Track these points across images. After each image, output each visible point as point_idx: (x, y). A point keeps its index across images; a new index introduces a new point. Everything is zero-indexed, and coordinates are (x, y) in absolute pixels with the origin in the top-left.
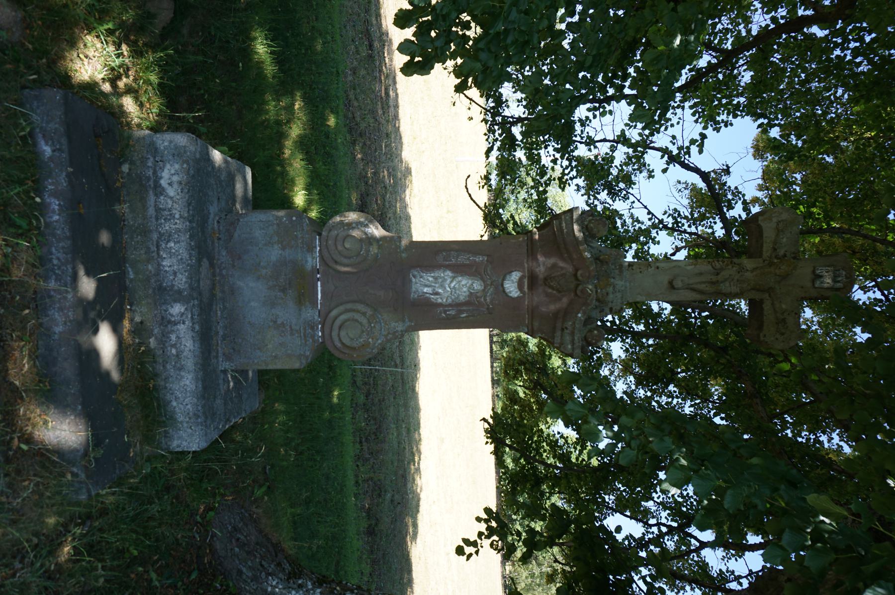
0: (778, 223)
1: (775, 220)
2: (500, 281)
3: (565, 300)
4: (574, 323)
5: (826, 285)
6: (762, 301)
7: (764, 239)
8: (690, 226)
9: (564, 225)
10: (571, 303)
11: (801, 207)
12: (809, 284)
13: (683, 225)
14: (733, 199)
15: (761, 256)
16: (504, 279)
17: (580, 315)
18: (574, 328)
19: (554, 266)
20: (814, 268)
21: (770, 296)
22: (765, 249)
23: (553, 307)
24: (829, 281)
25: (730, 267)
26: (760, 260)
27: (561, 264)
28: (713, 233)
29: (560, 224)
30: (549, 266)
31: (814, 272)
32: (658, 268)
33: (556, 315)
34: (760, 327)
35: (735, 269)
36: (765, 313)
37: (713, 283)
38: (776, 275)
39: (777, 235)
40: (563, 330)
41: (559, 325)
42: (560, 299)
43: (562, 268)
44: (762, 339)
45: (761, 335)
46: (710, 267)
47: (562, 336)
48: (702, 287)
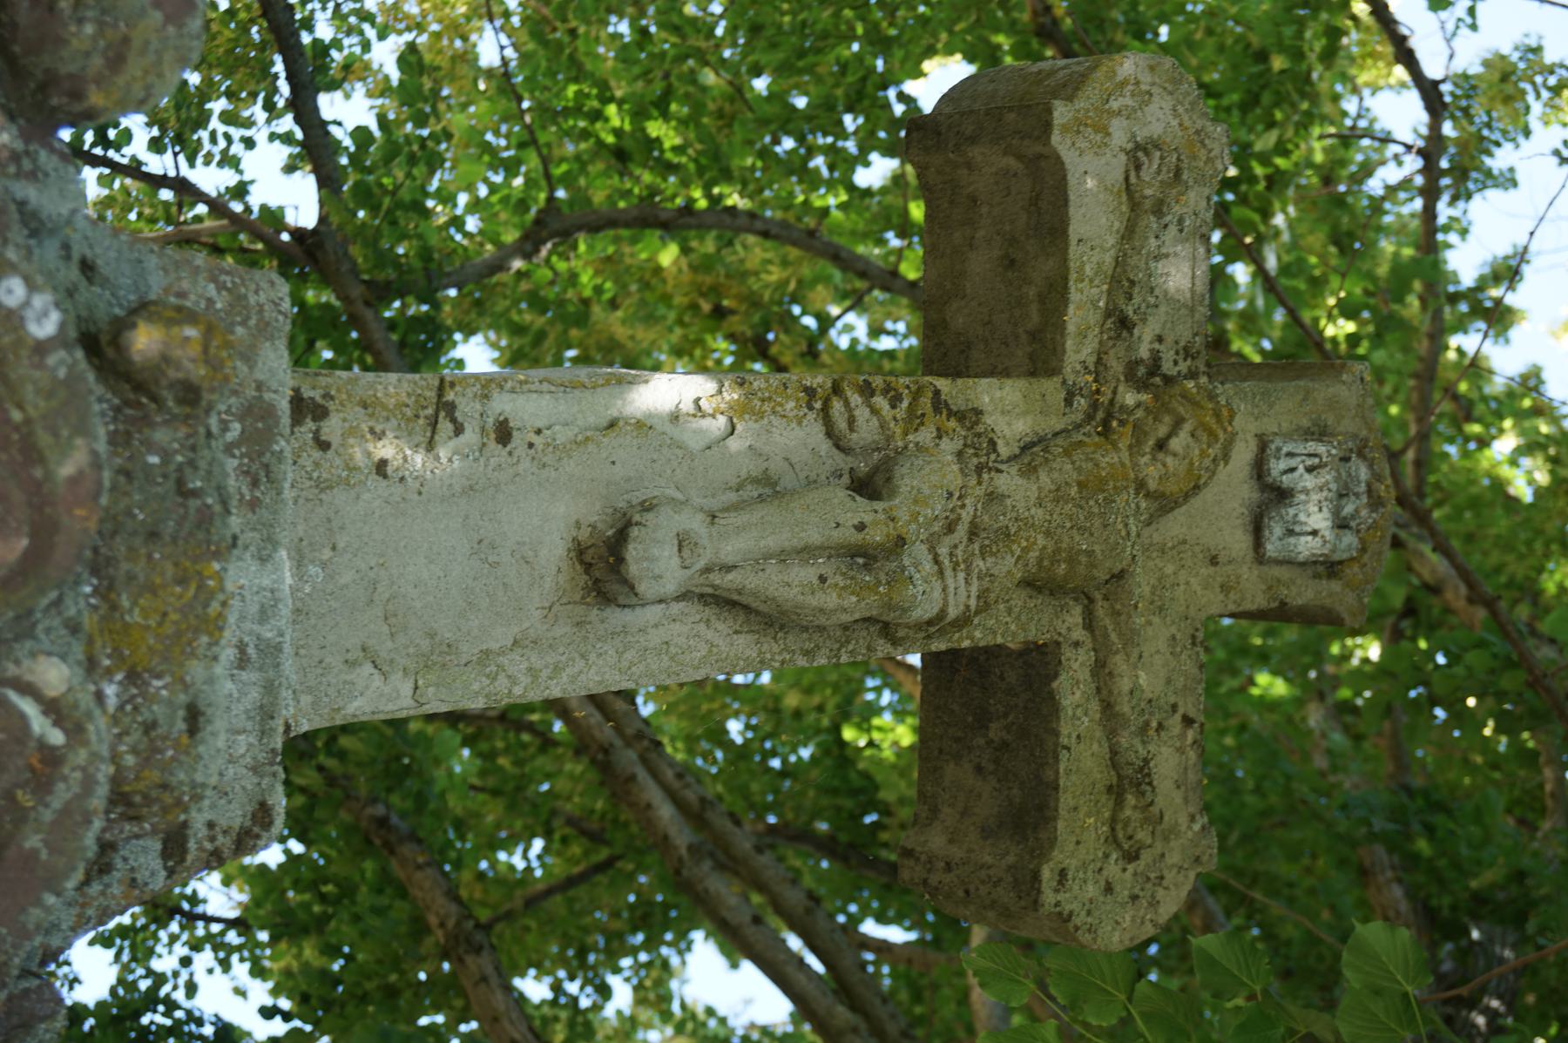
0: (1138, 152)
1: (1119, 134)
5: (1306, 547)
6: (1038, 663)
7: (1074, 251)
8: (156, 146)
11: (612, 110)
12: (1237, 541)
13: (127, 136)
14: (336, 44)
20: (1263, 444)
21: (1089, 624)
22: (1074, 317)
24: (1318, 519)
25: (926, 435)
26: (1051, 388)
28: (240, 191)
31: (1259, 468)
32: (504, 433)
34: (1029, 818)
35: (949, 446)
37: (861, 556)
38: (1141, 485)
39: (1129, 232)
44: (1049, 897)
45: (1046, 873)
46: (812, 433)
48: (792, 585)
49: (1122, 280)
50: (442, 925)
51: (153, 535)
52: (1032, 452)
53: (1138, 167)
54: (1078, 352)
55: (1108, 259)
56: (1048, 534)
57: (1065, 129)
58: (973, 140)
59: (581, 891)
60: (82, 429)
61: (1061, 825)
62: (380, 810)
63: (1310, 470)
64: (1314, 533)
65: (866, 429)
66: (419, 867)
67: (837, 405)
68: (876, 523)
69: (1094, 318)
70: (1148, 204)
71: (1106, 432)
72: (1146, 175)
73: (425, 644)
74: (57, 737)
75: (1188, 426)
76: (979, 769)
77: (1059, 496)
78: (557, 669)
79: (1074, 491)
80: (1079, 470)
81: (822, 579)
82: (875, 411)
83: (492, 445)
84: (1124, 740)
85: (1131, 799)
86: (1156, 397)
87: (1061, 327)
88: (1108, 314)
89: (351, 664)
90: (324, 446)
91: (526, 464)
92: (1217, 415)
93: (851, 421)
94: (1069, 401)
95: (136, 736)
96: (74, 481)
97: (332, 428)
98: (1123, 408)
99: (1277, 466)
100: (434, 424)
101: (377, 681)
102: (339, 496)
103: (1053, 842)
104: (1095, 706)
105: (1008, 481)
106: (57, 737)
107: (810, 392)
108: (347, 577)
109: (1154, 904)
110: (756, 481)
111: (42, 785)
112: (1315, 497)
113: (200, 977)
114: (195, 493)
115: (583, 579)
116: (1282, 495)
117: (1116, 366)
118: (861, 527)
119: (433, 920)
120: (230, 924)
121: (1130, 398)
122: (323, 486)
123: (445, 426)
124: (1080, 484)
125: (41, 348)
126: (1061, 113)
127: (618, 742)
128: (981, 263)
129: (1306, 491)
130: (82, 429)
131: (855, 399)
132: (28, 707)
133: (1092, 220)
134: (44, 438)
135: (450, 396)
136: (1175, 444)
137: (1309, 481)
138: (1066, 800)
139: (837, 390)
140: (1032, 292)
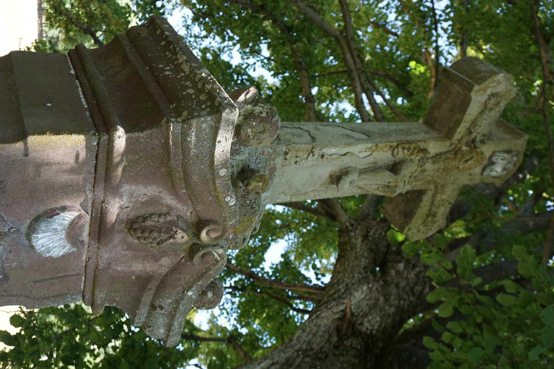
2: (24, 229)
3: (166, 262)
4: (178, 302)
9: (193, 138)
10: (175, 269)
15: (448, 136)
16: (32, 229)
17: (190, 293)
18: (176, 309)
19: (153, 201)
23: (138, 267)
26: (448, 143)
27: (169, 200)
29: (185, 134)
30: (143, 199)
33: (144, 281)
36: (422, 205)
40: (153, 307)
41: (147, 298)
42: (156, 259)
43: (170, 208)
47: (149, 315)
49: (474, 123)
50: (306, 93)
51: (245, 215)
52: (437, 157)
53: (490, 99)
54: (457, 136)
55: (474, 117)
56: (432, 177)
57: (476, 91)
58: (456, 82)
59: (340, 75)
60: (235, 218)
61: (413, 221)
62: (301, 60)
63: (502, 159)
64: (497, 172)
65: (401, 155)
66: (305, 77)
67: (396, 150)
68: (393, 182)
69: (464, 129)
70: (488, 108)
71: (456, 154)
72: (491, 102)
73: (295, 191)
74: (219, 259)
75: (474, 159)
76: (403, 200)
77: (437, 170)
78: (319, 195)
79: (441, 171)
80: (445, 166)
81: (378, 188)
82: (403, 153)
83: (320, 158)
84: (433, 208)
85: (430, 218)
86: (470, 150)
87: (456, 131)
88: (468, 129)
89: (280, 194)
90: (286, 159)
91: (325, 162)
92: (482, 158)
93: (398, 154)
94: (450, 146)
95: (234, 244)
96: (231, 225)
97: (288, 157)
98: (462, 151)
99: (494, 159)
100: (309, 155)
101: (284, 196)
102: (286, 167)
103: (410, 222)
104: (430, 201)
105: (429, 166)
106: (219, 259)
107: (391, 146)
108: (283, 180)
109: (427, 233)
110: (373, 163)
111: (214, 265)
112: (501, 165)
113: (257, 68)
114: (254, 208)
115: (330, 180)
116: (493, 163)
117: (465, 140)
118: (389, 182)
119: (304, 90)
120: (265, 58)
121: (464, 148)
122: (283, 166)
123: (311, 155)
124: (444, 170)
125: (231, 206)
126: (476, 88)
127: (354, 70)
128: (446, 106)
129: (499, 163)
130: (235, 218)
131: (400, 149)
132: (215, 254)
133: (473, 110)
134: (228, 219)
135: (314, 150)
136: (469, 162)
137: (501, 162)
138: (416, 216)
139: (397, 147)
140: (453, 119)
